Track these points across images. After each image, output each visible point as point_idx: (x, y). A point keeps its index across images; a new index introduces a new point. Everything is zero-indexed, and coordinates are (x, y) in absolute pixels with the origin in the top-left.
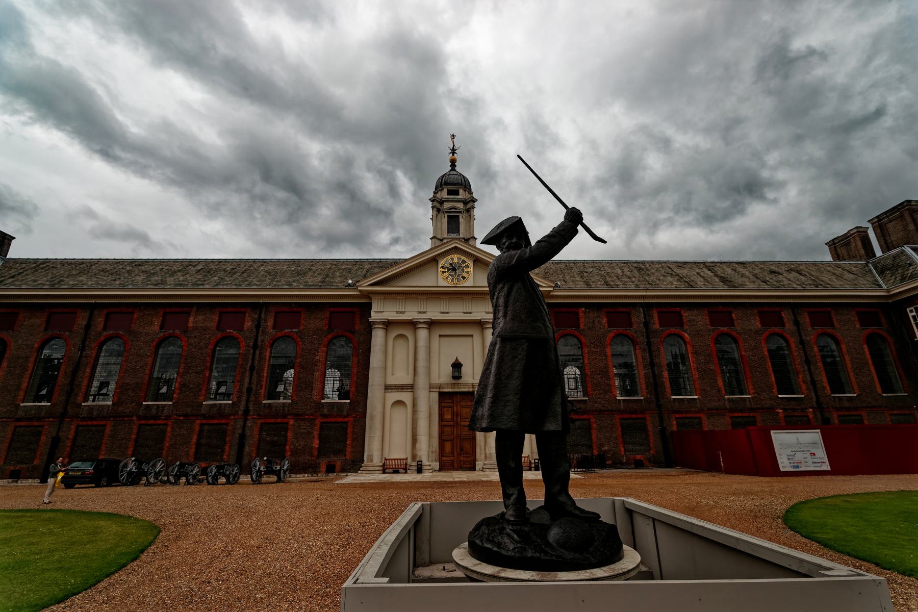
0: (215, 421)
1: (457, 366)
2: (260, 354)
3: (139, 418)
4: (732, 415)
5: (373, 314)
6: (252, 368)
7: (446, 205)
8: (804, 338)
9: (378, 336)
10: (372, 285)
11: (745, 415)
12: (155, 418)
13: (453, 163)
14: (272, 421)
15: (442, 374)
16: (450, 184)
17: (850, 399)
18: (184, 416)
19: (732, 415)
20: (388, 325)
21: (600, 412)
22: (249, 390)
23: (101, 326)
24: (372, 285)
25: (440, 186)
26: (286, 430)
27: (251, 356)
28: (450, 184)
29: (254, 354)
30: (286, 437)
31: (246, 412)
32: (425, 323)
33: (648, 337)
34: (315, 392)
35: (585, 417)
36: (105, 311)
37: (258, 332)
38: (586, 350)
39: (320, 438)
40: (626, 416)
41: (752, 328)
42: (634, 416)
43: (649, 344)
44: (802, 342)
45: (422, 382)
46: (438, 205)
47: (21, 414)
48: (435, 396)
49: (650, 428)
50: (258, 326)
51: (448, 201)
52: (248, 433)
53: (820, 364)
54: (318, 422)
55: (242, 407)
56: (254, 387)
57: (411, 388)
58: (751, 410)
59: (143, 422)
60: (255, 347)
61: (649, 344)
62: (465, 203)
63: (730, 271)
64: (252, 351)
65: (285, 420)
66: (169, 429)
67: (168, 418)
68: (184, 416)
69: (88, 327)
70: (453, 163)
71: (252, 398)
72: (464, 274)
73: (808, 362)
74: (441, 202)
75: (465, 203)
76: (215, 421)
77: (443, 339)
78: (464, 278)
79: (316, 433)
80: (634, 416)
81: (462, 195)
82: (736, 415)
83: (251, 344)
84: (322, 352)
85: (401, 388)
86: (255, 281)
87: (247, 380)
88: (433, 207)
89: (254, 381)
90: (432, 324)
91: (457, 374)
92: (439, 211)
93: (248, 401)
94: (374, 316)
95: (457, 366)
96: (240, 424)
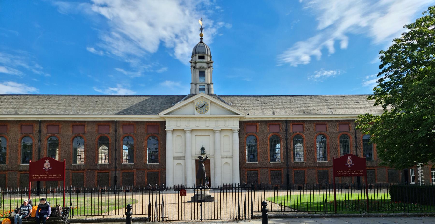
0: (104, 172)
1: (203, 149)
2: (119, 144)
3: (71, 170)
4: (318, 169)
5: (166, 127)
6: (116, 150)
7: (198, 65)
8: (357, 136)
9: (169, 136)
10: (166, 114)
11: (324, 169)
12: (78, 170)
13: (201, 39)
14: (127, 171)
15: (197, 152)
16: (199, 53)
17: (372, 162)
18: (90, 169)
19: (318, 169)
20: (174, 131)
21: (262, 168)
22: (116, 159)
23: (46, 132)
24: (166, 114)
25: (194, 53)
26: (133, 175)
27: (114, 145)
28: (199, 53)
29: (116, 143)
30: (133, 177)
31: (116, 168)
32: (189, 131)
33: (287, 136)
34: (144, 160)
35: (256, 170)
36: (46, 124)
37: (116, 134)
38: (258, 142)
39: (147, 178)
40: (273, 170)
41: (334, 131)
42: (277, 169)
43: (287, 139)
44: (356, 138)
45: (188, 156)
46: (193, 64)
47: (21, 169)
48: (194, 161)
49: (283, 175)
50: (116, 131)
51: (199, 62)
52: (117, 176)
53: (362, 148)
54: (146, 171)
55: (114, 166)
56: (118, 157)
57: (184, 158)
58: (328, 167)
59: (74, 172)
60: (116, 140)
61: (287, 139)
62: (208, 63)
63: (335, 102)
64: (114, 143)
65: (132, 171)
66: (85, 175)
67: (84, 170)
68: (90, 169)
69: (40, 132)
70: (201, 39)
71: (117, 162)
72: (206, 109)
73: (356, 147)
74: (196, 63)
75: (208, 63)
76: (104, 172)
77: (197, 137)
78: (206, 110)
79: (146, 176)
80: (277, 169)
81: (207, 59)
82: (320, 169)
83: (114, 139)
84: (145, 143)
85: (179, 158)
86: (110, 109)
87: (114, 155)
88: (191, 66)
89: (117, 155)
90: (192, 131)
91: (203, 152)
92: (194, 67)
93: (116, 164)
94: (167, 128)
95: (203, 149)
96: (114, 172)
